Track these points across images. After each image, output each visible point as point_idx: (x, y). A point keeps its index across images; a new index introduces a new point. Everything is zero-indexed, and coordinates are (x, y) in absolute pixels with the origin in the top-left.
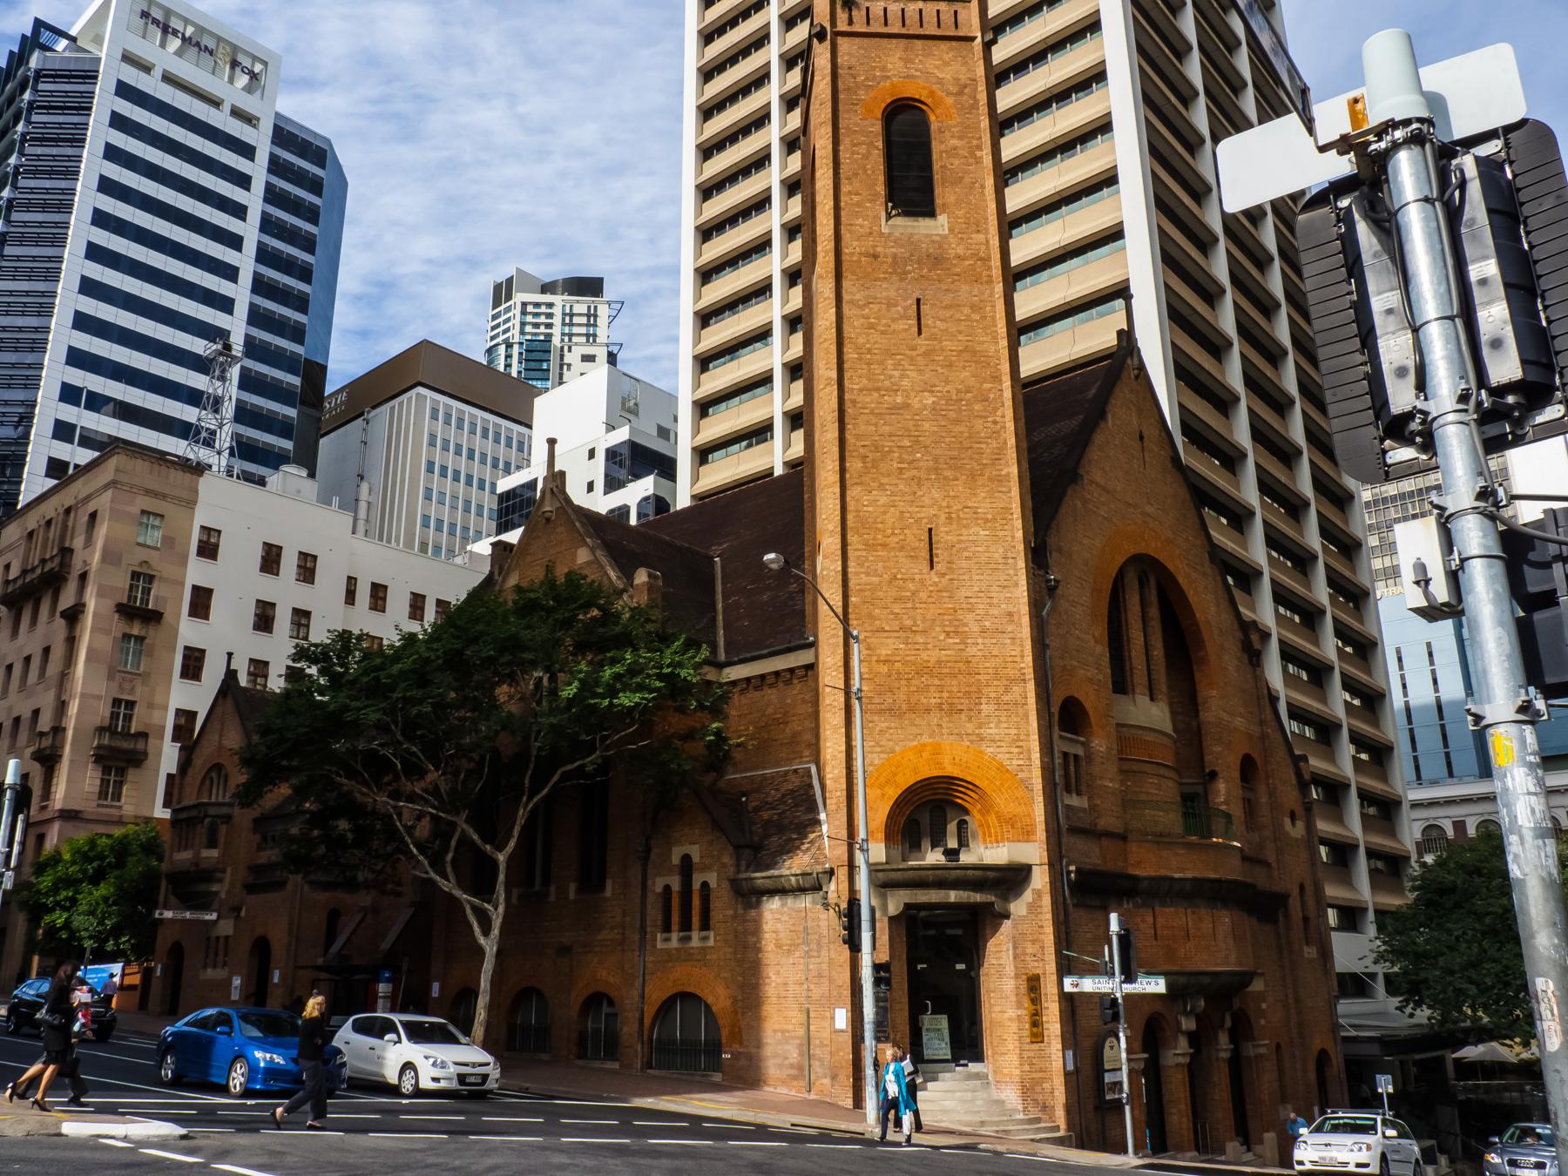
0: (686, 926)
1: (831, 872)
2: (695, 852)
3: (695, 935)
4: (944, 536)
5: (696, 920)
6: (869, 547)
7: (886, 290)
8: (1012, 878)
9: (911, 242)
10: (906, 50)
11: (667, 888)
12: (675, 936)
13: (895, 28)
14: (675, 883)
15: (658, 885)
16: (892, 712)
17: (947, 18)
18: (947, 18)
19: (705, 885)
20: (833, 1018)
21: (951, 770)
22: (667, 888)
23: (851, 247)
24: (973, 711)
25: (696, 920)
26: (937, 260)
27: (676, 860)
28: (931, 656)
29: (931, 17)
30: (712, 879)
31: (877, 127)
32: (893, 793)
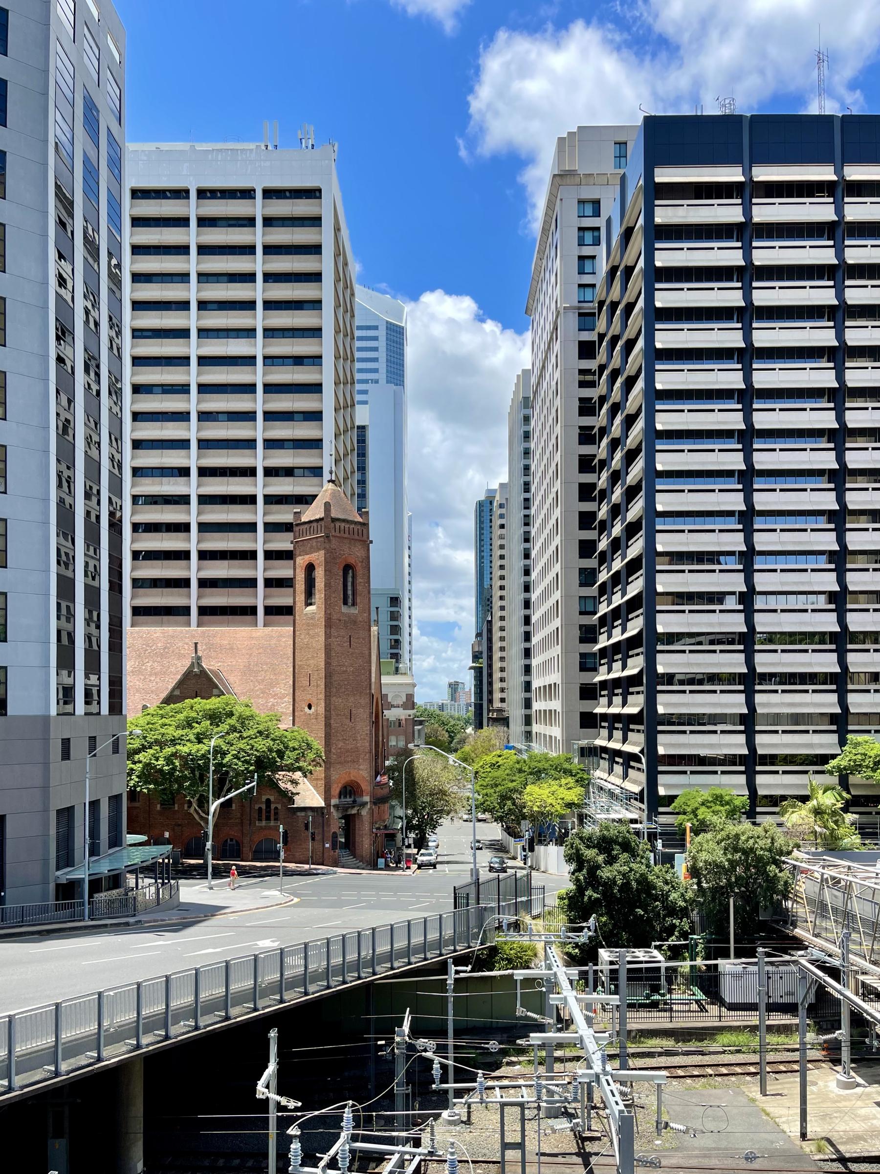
0: (268, 819)
2: (272, 798)
3: (272, 823)
4: (353, 712)
6: (337, 715)
7: (342, 632)
9: (348, 615)
10: (350, 543)
11: (260, 809)
12: (264, 823)
13: (346, 535)
14: (264, 807)
15: (257, 807)
16: (340, 763)
17: (360, 531)
18: (360, 531)
19: (276, 808)
20: (324, 845)
21: (353, 778)
22: (260, 809)
23: (335, 617)
24: (358, 761)
25: (272, 818)
26: (355, 622)
27: (264, 798)
28: (349, 747)
30: (279, 806)
32: (340, 785)
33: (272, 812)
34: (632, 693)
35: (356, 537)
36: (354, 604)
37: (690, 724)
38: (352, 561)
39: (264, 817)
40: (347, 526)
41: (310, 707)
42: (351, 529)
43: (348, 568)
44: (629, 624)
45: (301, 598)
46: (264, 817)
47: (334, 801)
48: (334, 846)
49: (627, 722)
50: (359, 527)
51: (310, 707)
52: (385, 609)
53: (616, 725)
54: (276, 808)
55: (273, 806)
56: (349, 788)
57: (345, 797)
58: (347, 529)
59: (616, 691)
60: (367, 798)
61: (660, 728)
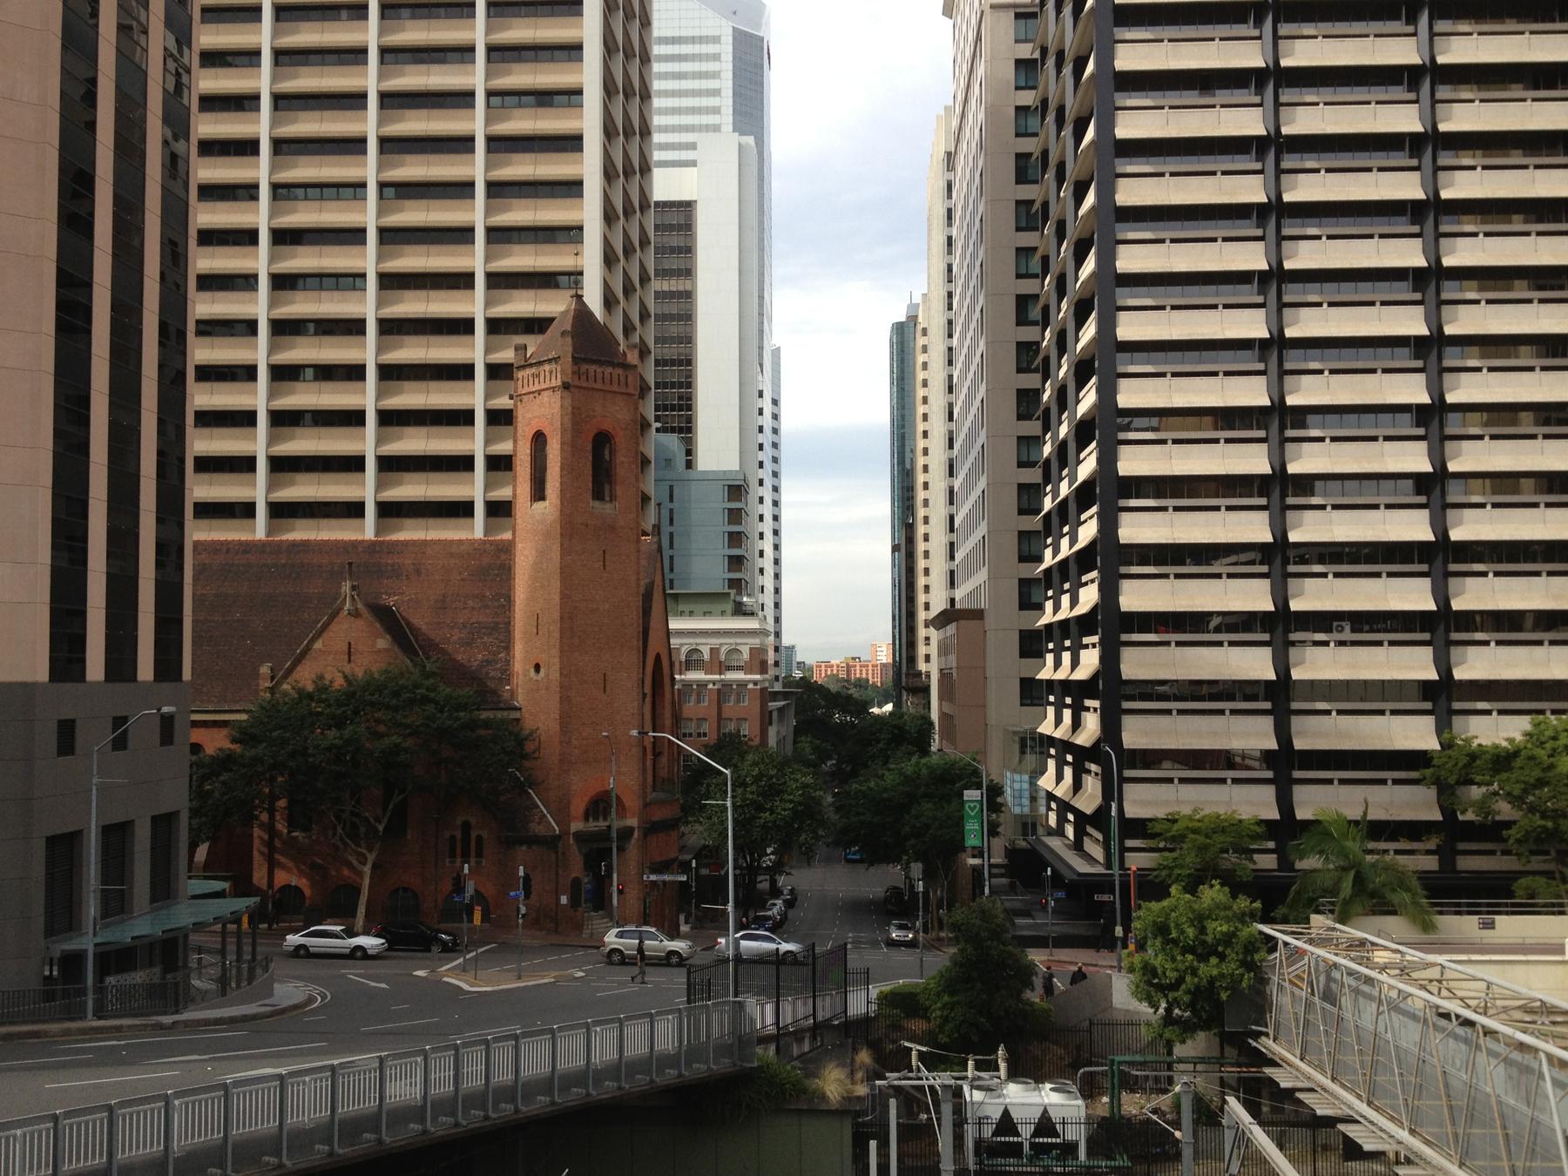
1: (559, 837)
2: (473, 821)
5: (473, 853)
8: (626, 834)
13: (599, 385)
15: (447, 834)
19: (479, 838)
20: (558, 899)
22: (453, 838)
25: (473, 853)
26: (612, 528)
27: (459, 822)
29: (615, 380)
30: (485, 834)
31: (589, 447)
32: (586, 799)
33: (473, 843)
34: (1086, 646)
35: (615, 388)
36: (613, 498)
37: (1177, 699)
38: (606, 426)
39: (459, 850)
40: (599, 370)
41: (537, 668)
42: (607, 376)
43: (602, 441)
44: (1081, 529)
45: (524, 487)
46: (459, 850)
47: (576, 826)
48: (575, 902)
49: (1076, 692)
50: (620, 371)
51: (537, 668)
52: (718, 502)
53: (1088, 703)
54: (479, 838)
55: (474, 834)
56: (602, 806)
57: (596, 819)
58: (599, 376)
59: (1086, 640)
60: (632, 822)
61: (1126, 705)
